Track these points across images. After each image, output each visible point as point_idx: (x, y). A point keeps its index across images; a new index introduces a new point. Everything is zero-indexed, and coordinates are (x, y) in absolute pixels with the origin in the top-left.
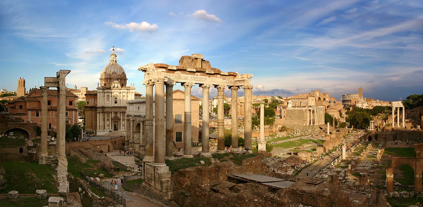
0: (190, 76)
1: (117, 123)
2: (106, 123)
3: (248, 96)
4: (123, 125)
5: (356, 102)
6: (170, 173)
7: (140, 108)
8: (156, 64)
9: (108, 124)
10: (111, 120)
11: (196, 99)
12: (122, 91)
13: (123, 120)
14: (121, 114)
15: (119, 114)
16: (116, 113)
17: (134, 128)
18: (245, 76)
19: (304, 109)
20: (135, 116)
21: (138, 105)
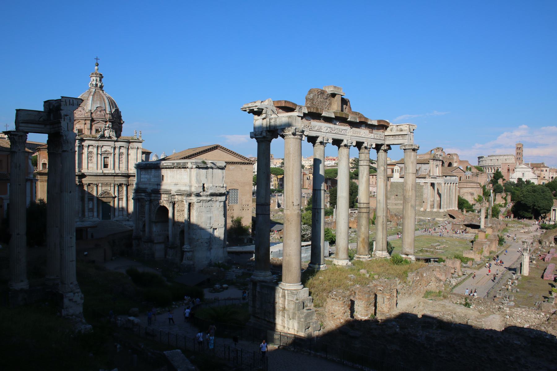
2: (86, 205)
3: (412, 163)
5: (509, 170)
9: (91, 206)
11: (247, 162)
12: (118, 144)
15: (112, 188)
19: (422, 181)
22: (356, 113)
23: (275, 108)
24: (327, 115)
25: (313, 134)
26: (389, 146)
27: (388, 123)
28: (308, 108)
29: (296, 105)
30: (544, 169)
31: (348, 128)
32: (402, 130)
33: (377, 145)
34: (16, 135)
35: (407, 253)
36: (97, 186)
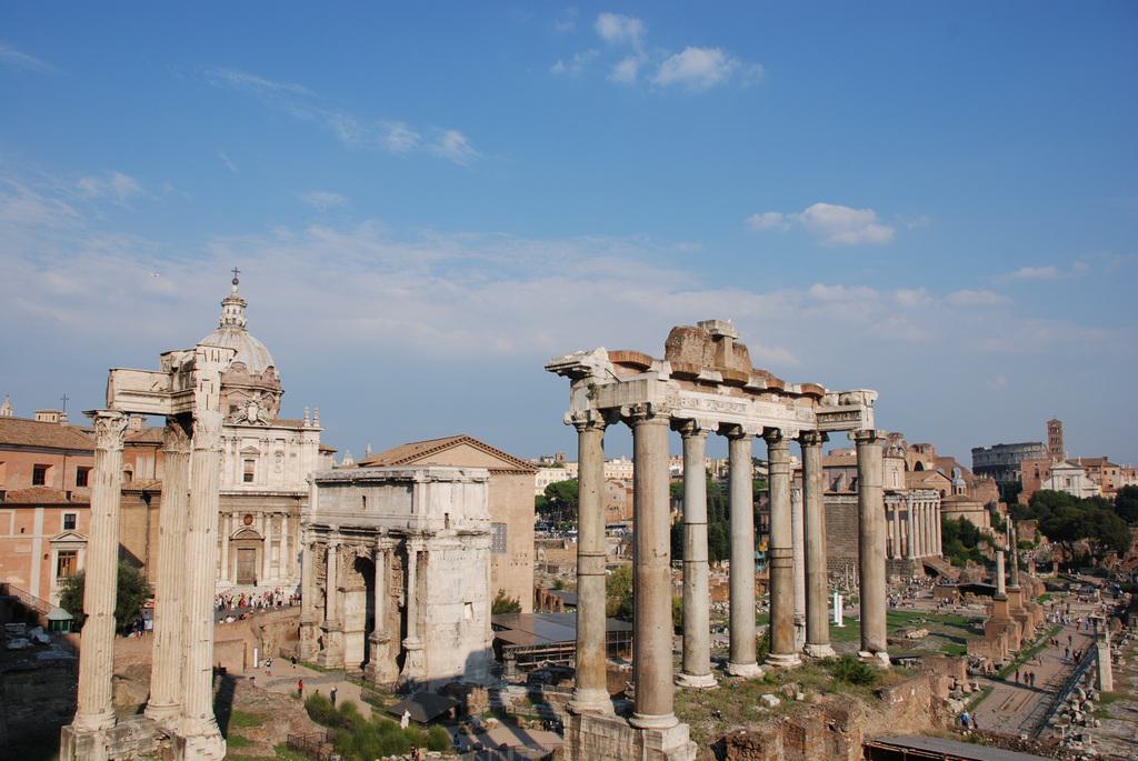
0: (703, 396)
1: (249, 554)
4: (272, 562)
5: (1037, 475)
6: (694, 747)
7: (368, 501)
8: (617, 353)
10: (230, 546)
12: (273, 435)
13: (276, 543)
14: (269, 521)
16: (248, 517)
17: (340, 576)
18: (857, 399)
20: (347, 531)
21: (361, 491)
22: (759, 373)
23: (611, 367)
24: (709, 378)
25: (683, 414)
26: (824, 434)
27: (822, 390)
28: (674, 364)
29: (651, 359)
30: (1110, 470)
31: (746, 400)
32: (848, 403)
33: (802, 433)
34: (108, 418)
35: (872, 647)
36: (231, 516)
